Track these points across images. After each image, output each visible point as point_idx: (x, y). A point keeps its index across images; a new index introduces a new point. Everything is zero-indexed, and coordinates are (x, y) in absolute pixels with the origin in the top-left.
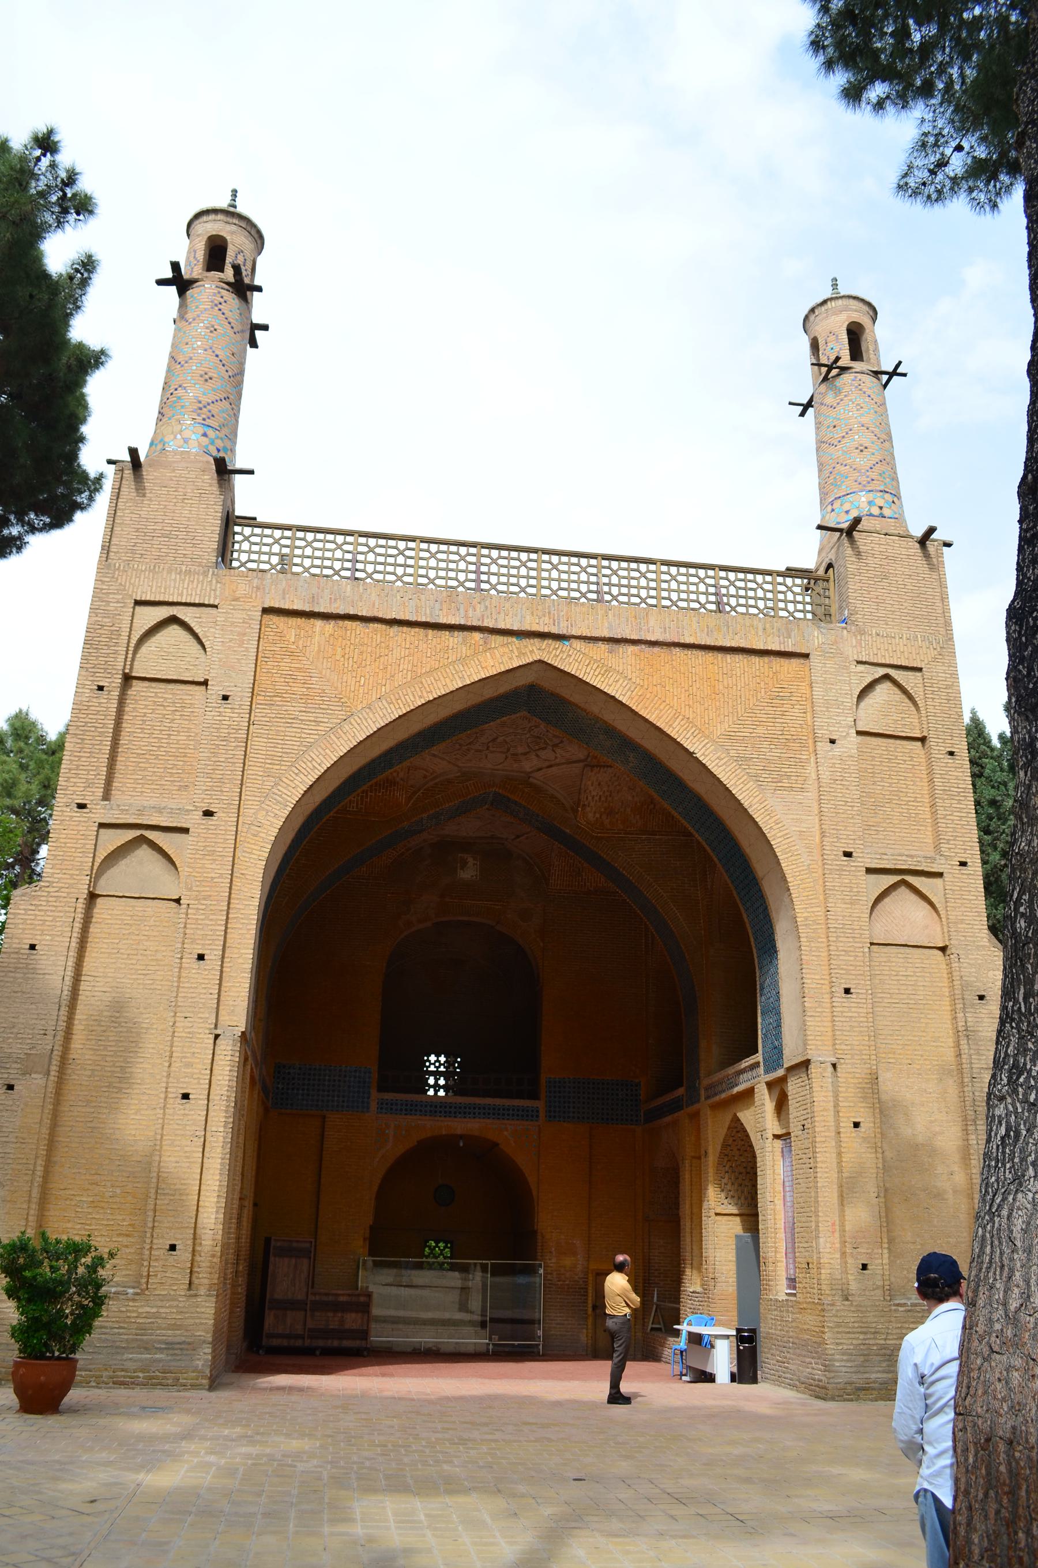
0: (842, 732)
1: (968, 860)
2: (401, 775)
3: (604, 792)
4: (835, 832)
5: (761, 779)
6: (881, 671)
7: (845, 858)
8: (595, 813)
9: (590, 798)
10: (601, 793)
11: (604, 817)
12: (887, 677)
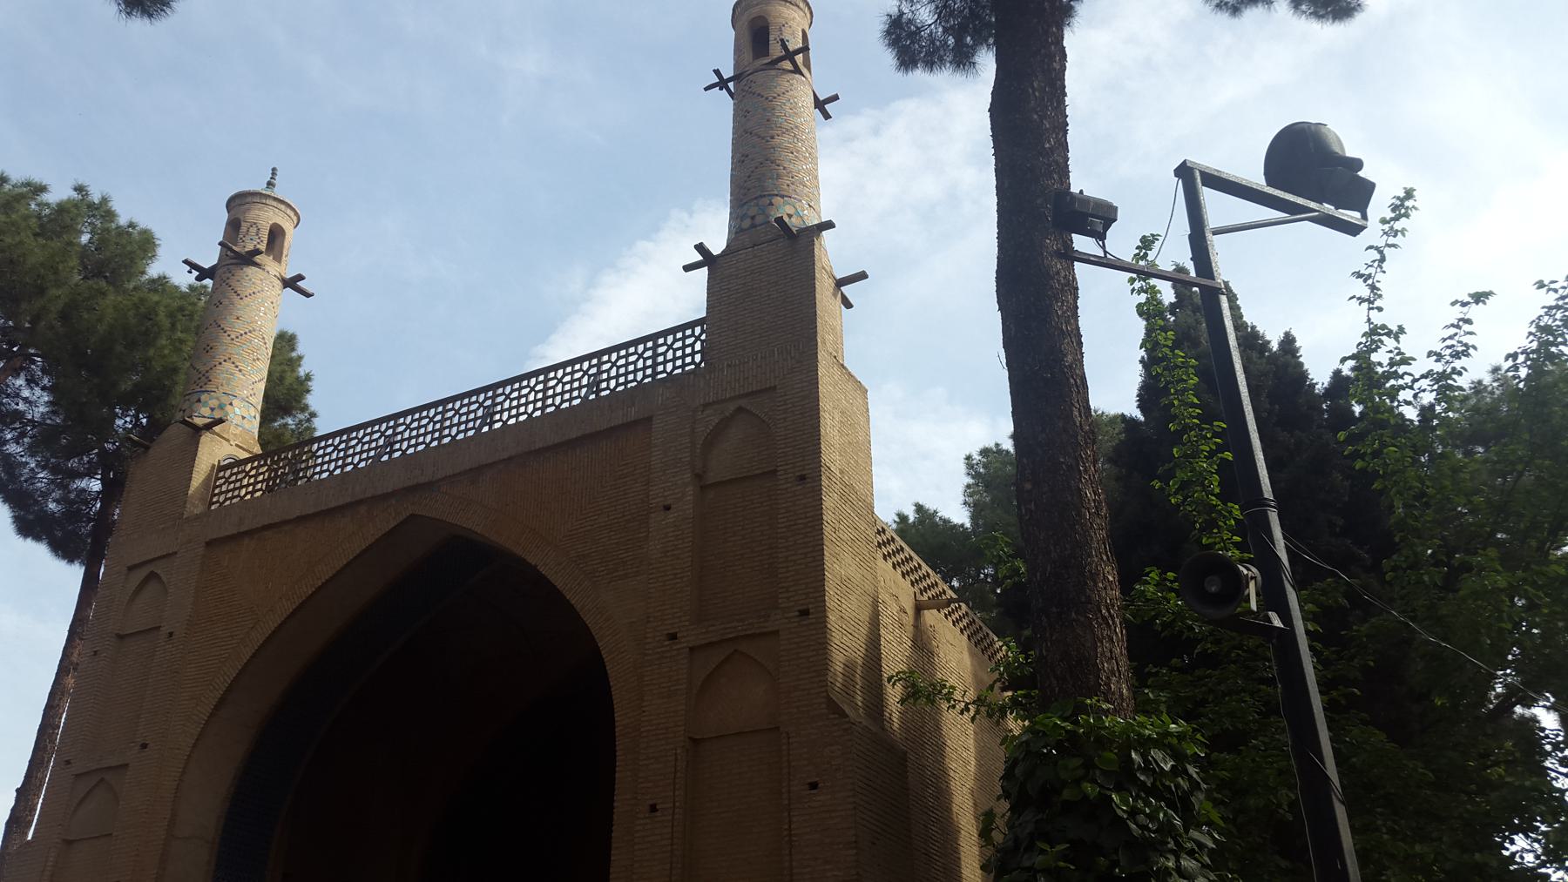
0: (678, 493)
1: (810, 606)
4: (659, 614)
5: (597, 574)
6: (732, 407)
7: (667, 643)
12: (740, 409)
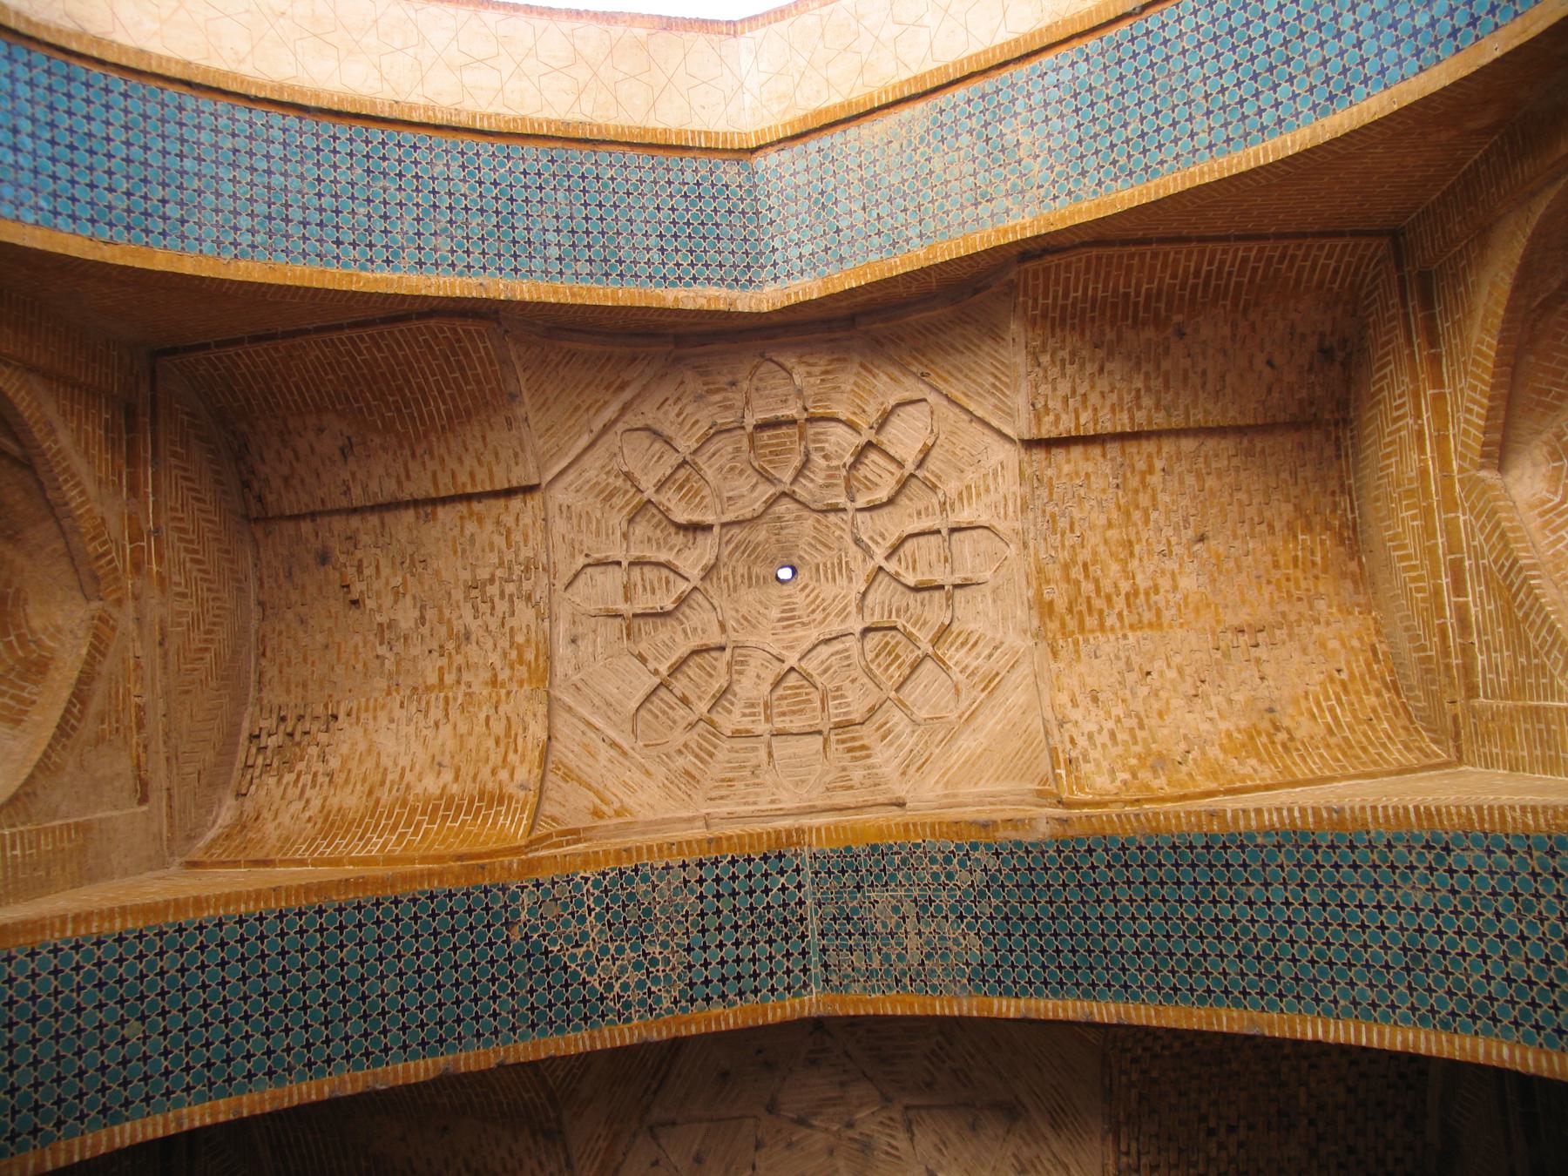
2: (521, 774)
3: (1118, 720)
8: (1112, 771)
9: (1082, 742)
10: (1110, 724)
11: (1145, 775)
